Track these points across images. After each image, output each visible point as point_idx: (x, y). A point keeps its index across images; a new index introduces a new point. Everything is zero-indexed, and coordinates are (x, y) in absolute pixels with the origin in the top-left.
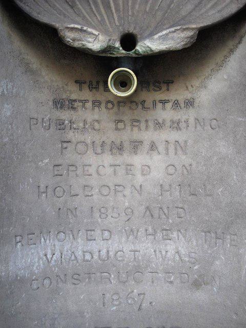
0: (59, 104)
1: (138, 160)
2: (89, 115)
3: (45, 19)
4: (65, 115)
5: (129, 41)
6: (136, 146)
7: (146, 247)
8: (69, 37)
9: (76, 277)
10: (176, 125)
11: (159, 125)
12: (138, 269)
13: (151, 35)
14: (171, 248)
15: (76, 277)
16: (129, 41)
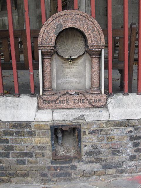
0: (63, 63)
1: (72, 69)
2: (66, 64)
3: (61, 55)
4: (63, 64)
5: (71, 57)
6: (72, 68)
7: (73, 79)
8: (64, 57)
9: (65, 83)
10: (76, 65)
11: (74, 65)
12: (72, 82)
13: (73, 56)
14: (76, 79)
15: (65, 83)
16: (71, 57)
